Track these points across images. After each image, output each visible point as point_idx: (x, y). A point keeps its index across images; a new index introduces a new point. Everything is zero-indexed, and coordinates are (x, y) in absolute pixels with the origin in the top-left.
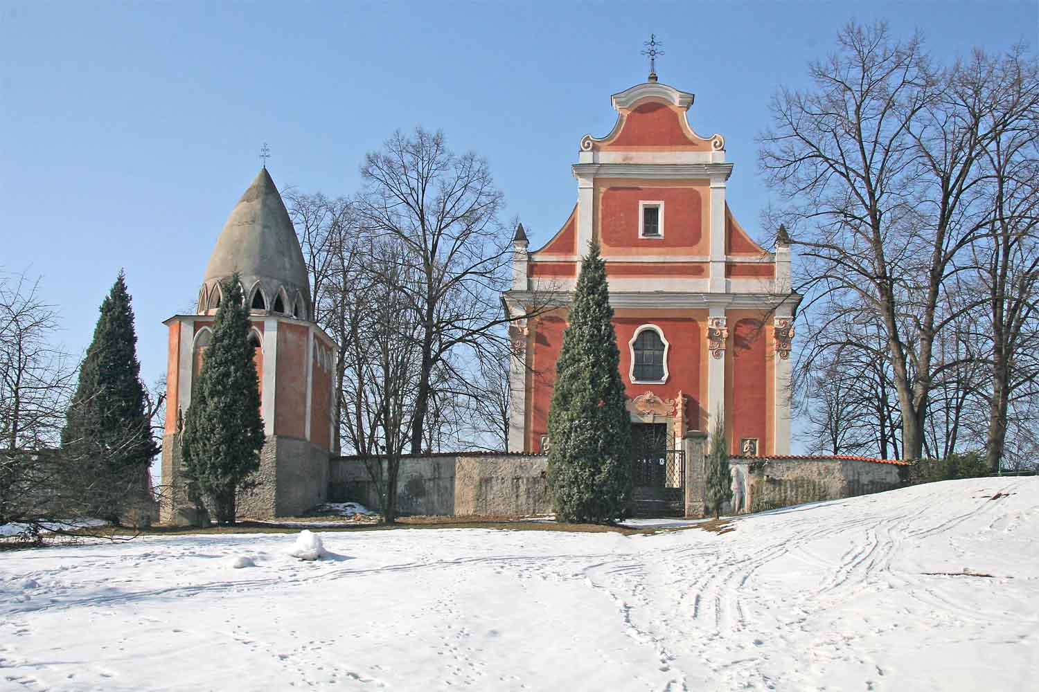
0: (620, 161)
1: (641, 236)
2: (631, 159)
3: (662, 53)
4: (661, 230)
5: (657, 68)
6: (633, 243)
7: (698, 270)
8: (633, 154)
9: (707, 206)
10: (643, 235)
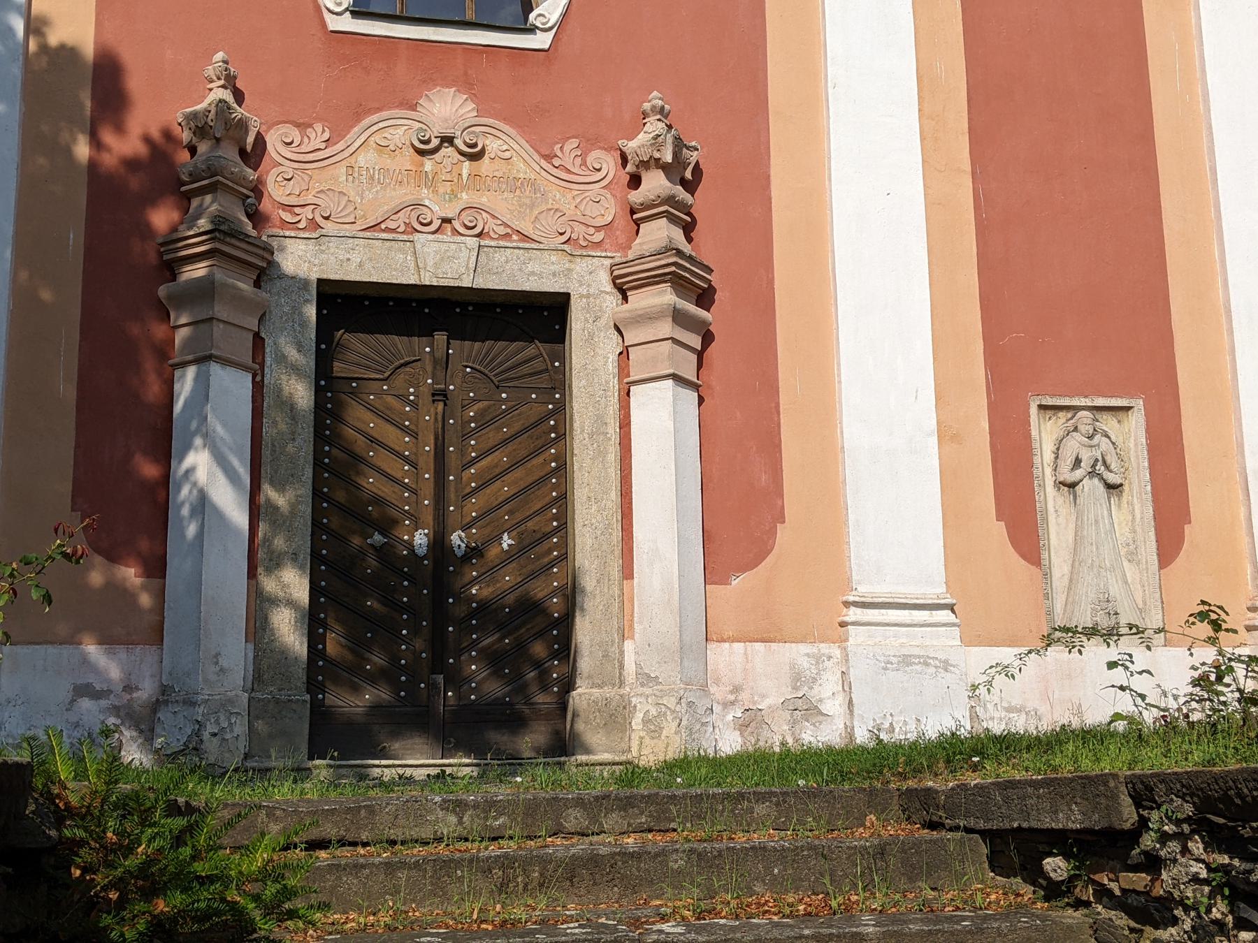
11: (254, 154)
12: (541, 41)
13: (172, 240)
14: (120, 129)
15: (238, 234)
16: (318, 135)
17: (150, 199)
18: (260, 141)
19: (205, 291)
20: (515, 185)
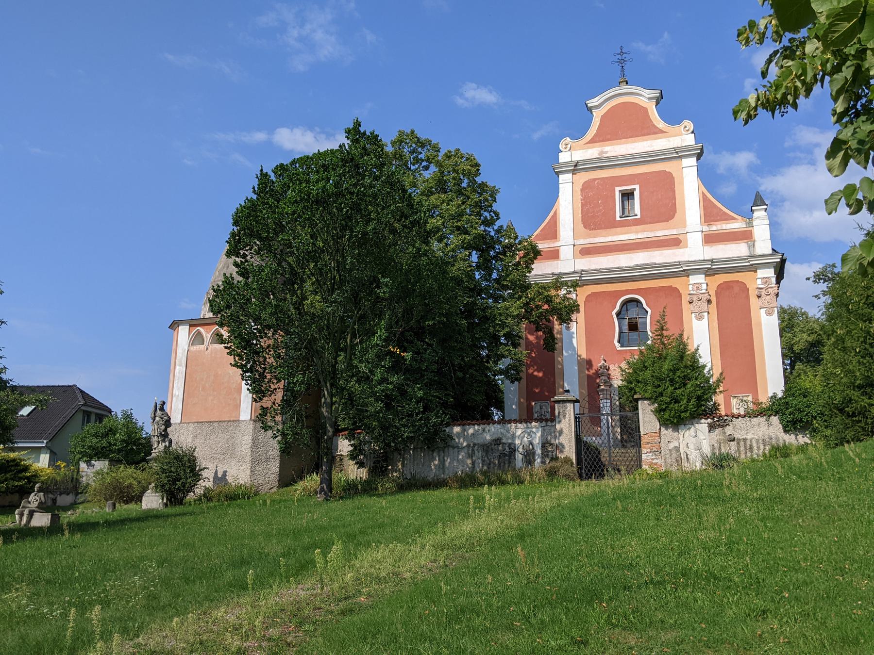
0: (596, 155)
1: (618, 218)
2: (607, 152)
4: (637, 210)
6: (611, 224)
7: (675, 242)
8: (607, 149)
9: (682, 183)
10: (621, 217)
11: (608, 370)
13: (599, 383)
14: (592, 369)
15: (607, 382)
17: (596, 379)
18: (609, 367)
19: (603, 390)
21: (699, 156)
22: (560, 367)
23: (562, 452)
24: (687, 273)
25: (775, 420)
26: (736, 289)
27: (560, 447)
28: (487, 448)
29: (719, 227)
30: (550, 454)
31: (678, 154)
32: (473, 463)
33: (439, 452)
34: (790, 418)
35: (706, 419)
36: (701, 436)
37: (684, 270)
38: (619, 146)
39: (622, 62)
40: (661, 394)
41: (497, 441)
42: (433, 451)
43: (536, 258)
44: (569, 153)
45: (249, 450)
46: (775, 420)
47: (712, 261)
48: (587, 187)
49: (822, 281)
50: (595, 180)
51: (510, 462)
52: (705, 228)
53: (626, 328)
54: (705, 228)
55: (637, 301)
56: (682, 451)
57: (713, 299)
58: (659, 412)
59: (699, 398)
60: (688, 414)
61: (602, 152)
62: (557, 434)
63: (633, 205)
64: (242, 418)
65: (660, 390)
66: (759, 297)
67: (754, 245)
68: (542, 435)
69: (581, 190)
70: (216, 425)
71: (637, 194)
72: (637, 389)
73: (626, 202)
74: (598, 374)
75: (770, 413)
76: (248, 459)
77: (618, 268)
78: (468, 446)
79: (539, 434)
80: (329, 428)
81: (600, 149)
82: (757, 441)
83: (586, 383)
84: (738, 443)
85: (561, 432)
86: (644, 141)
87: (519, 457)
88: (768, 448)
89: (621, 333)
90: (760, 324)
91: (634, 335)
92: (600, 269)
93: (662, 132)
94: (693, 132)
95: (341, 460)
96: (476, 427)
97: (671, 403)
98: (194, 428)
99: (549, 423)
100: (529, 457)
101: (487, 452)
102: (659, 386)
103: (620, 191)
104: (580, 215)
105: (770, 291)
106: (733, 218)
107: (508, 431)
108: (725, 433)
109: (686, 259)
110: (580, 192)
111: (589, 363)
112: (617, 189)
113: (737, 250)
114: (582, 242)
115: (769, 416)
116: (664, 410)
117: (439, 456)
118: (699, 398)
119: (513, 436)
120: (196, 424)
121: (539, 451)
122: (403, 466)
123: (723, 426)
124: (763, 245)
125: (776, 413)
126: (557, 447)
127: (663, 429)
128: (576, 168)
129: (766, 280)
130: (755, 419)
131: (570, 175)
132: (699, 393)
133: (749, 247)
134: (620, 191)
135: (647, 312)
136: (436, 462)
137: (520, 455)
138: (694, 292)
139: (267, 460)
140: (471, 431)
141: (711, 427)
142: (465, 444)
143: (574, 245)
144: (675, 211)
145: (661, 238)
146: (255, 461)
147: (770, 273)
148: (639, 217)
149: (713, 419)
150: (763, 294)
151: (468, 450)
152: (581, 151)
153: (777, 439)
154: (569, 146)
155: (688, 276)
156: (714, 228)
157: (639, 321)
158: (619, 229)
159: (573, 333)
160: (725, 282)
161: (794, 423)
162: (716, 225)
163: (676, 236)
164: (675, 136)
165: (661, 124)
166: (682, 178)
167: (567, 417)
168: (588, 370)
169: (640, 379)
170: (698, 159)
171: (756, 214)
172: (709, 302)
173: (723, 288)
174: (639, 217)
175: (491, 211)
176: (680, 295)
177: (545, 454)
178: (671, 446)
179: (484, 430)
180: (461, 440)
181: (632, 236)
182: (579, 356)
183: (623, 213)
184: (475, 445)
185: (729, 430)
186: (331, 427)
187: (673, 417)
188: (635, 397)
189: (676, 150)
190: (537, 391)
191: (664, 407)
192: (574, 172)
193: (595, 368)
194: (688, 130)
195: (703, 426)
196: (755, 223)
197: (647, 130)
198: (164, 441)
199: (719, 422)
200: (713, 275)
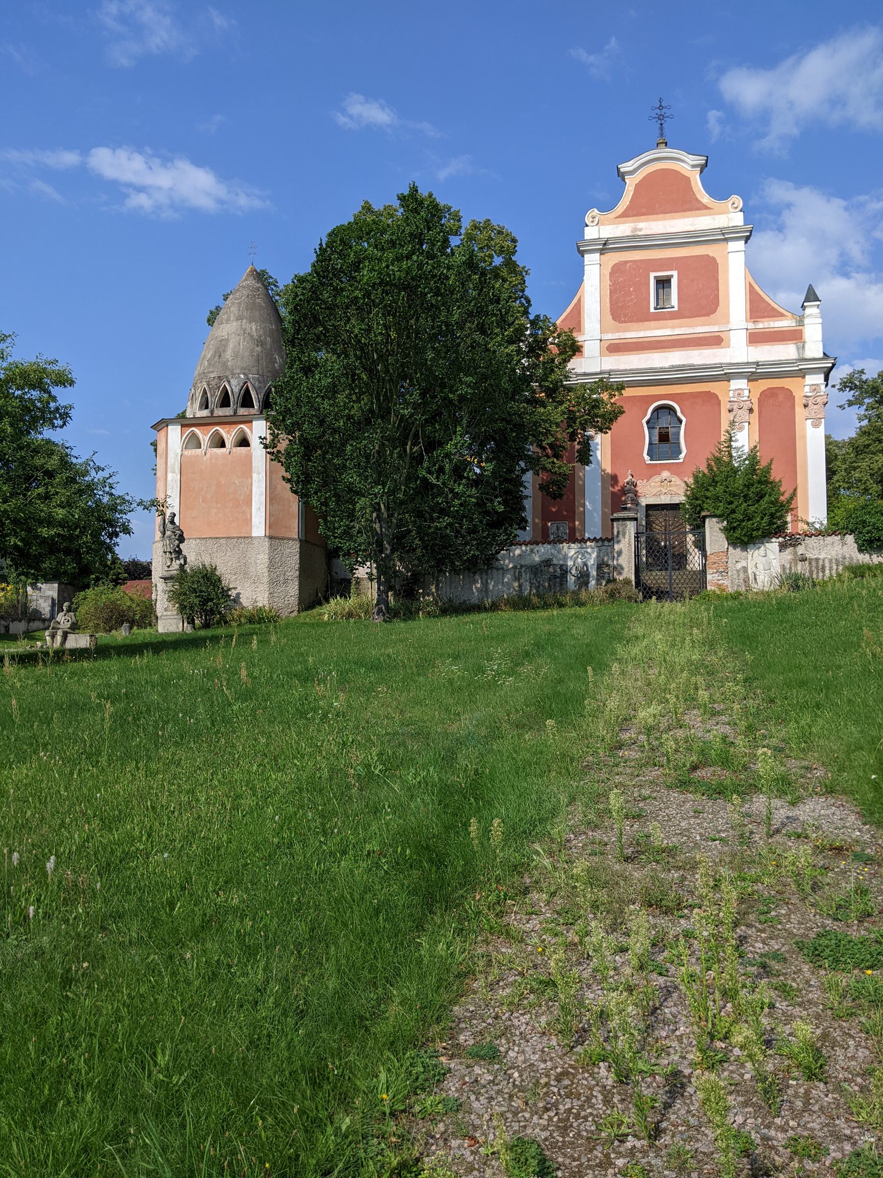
0: (628, 233)
1: (652, 310)
2: (641, 230)
3: (671, 117)
5: (665, 131)
6: (644, 317)
7: (716, 341)
8: (641, 225)
9: (727, 271)
10: (655, 309)
11: (635, 486)
12: (681, 461)
16: (645, 481)
20: (677, 485)
21: (747, 239)
22: (581, 483)
23: (620, 573)
24: (728, 377)
25: (850, 539)
26: (781, 397)
27: (619, 569)
28: (536, 570)
29: (766, 325)
30: (606, 575)
31: (724, 236)
32: (520, 586)
33: (481, 573)
34: (867, 537)
35: (777, 538)
36: (771, 556)
37: (726, 374)
38: (655, 223)
39: (661, 117)
40: (733, 511)
41: (547, 563)
42: (475, 573)
43: (574, 355)
44: (597, 228)
45: (266, 570)
46: (850, 539)
47: (757, 364)
48: (617, 270)
49: (848, 389)
50: (626, 262)
51: (561, 584)
52: (751, 326)
53: (656, 439)
54: (751, 326)
55: (670, 409)
56: (750, 572)
57: (756, 408)
58: (729, 531)
59: (772, 515)
60: (760, 533)
61: (635, 229)
62: (616, 555)
63: (669, 295)
64: (254, 535)
65: (733, 506)
66: (806, 406)
67: (803, 347)
68: (598, 556)
69: (611, 274)
70: (223, 541)
71: (674, 282)
72: (705, 506)
73: (661, 291)
74: (624, 492)
75: (845, 531)
76: (266, 580)
77: (652, 369)
78: (515, 567)
79: (594, 555)
80: (387, 546)
81: (633, 225)
82: (831, 561)
83: (610, 501)
84: (810, 563)
85: (620, 553)
86: (684, 217)
87: (571, 579)
88: (841, 568)
89: (650, 444)
90: (804, 437)
91: (665, 447)
92: (631, 370)
93: (706, 208)
94: (741, 211)
95: (358, 583)
96: (524, 548)
97: (743, 521)
98: (197, 545)
99: (606, 543)
100: (583, 578)
101: (536, 574)
102: (731, 503)
103: (655, 277)
104: (608, 305)
105: (819, 399)
106: (782, 315)
107: (559, 551)
108: (795, 553)
109: (728, 361)
110: (608, 276)
111: (614, 479)
112: (652, 275)
113: (786, 352)
114: (609, 336)
115: (844, 535)
116: (734, 529)
117: (481, 578)
118: (772, 515)
119: (565, 557)
120: (198, 541)
121: (594, 573)
122: (437, 590)
123: (795, 546)
124: (814, 348)
125: (852, 532)
126: (615, 568)
127: (731, 548)
128: (605, 247)
129: (815, 387)
130: (829, 538)
131: (597, 256)
132: (773, 510)
133: (798, 349)
134: (655, 277)
135: (680, 421)
136: (479, 585)
137: (573, 578)
138: (735, 399)
139: (286, 581)
140: (518, 552)
141: (783, 547)
142: (511, 566)
143: (601, 340)
144: (718, 304)
145: (701, 335)
146: (273, 582)
147: (819, 379)
148: (676, 309)
149: (784, 538)
150: (810, 403)
151: (515, 573)
152: (611, 226)
153: (851, 558)
154: (597, 219)
155: (729, 381)
156: (761, 326)
157: (671, 430)
158: (653, 323)
159: (597, 444)
160: (769, 389)
161: (870, 542)
162: (763, 322)
163: (717, 334)
164: (722, 214)
165: (705, 198)
166: (727, 265)
167: (627, 536)
168: (613, 486)
169: (708, 494)
170: (746, 243)
171: (808, 311)
172: (751, 410)
173: (766, 396)
174: (676, 309)
175: (522, 297)
176: (719, 403)
177: (600, 576)
178: (739, 566)
179: (532, 551)
180: (507, 561)
181: (668, 332)
182: (604, 471)
183: (657, 304)
184: (522, 566)
185: (800, 550)
186: (389, 544)
187: (744, 535)
188: (703, 514)
189: (722, 231)
190: (554, 510)
191: (735, 525)
192: (602, 252)
193: (621, 484)
194: (736, 208)
195: (773, 545)
196: (806, 321)
197: (690, 205)
198: (178, 558)
199: (791, 542)
200: (756, 380)
